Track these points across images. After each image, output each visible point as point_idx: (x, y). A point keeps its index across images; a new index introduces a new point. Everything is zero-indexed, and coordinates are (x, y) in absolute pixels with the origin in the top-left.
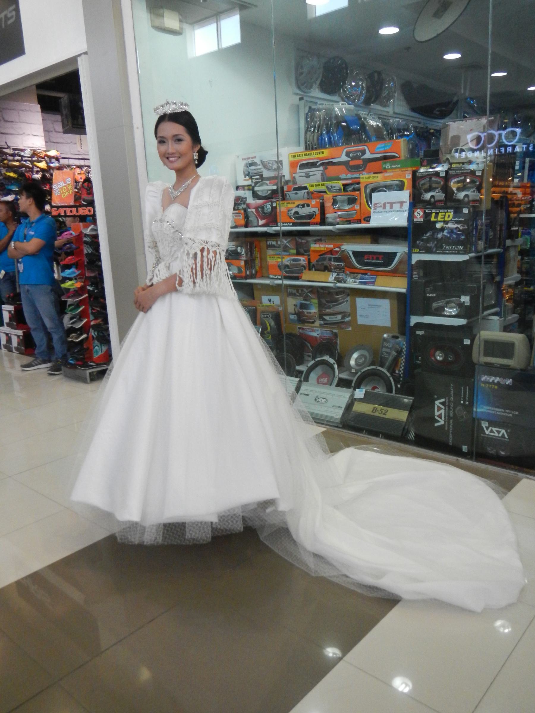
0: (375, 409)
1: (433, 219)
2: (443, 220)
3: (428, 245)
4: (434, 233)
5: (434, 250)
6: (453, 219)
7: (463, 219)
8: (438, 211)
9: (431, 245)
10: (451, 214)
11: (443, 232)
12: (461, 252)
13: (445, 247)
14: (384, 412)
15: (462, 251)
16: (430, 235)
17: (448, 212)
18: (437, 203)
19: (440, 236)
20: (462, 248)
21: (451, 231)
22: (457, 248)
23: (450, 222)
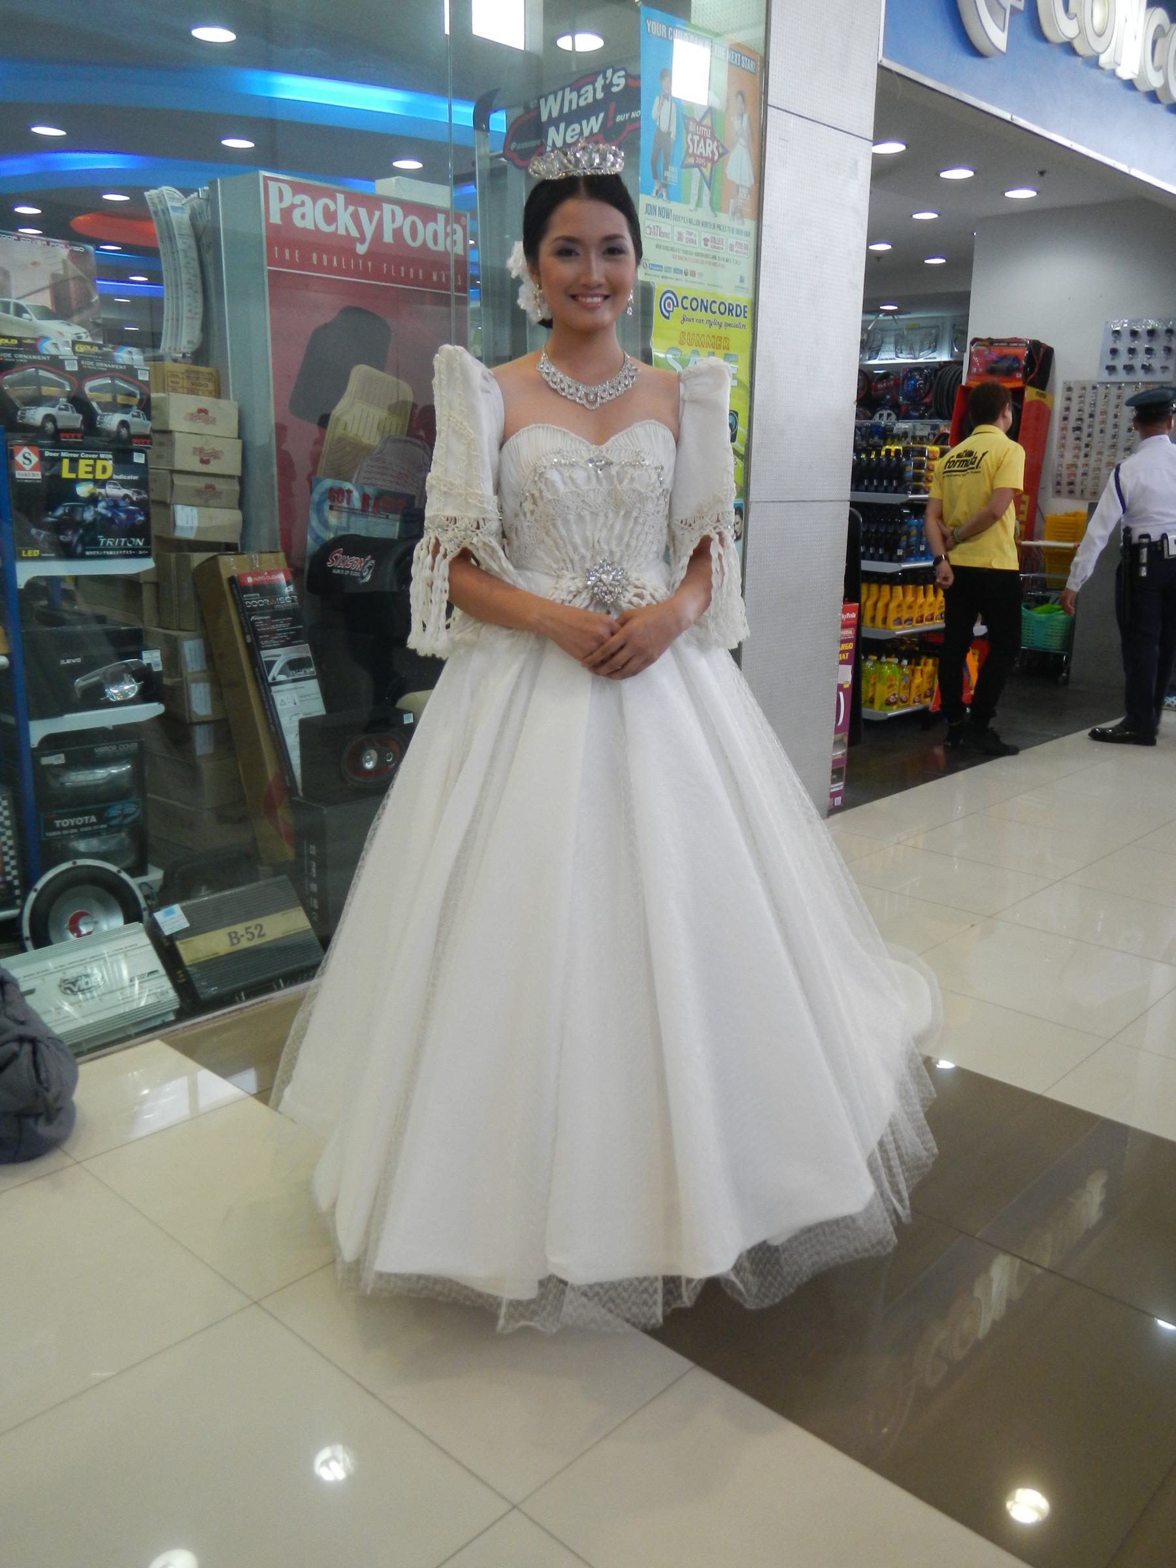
0: (233, 935)
1: (66, 474)
2: (90, 476)
3: (62, 537)
4: (72, 509)
5: (79, 549)
6: (115, 477)
7: (136, 478)
8: (77, 455)
9: (69, 537)
10: (109, 464)
11: (96, 506)
12: (140, 552)
13: (105, 543)
14: (256, 933)
15: (142, 549)
16: (65, 514)
17: (99, 458)
18: (62, 435)
19: (89, 515)
20: (141, 544)
21: (114, 504)
22: (131, 542)
23: (110, 483)
